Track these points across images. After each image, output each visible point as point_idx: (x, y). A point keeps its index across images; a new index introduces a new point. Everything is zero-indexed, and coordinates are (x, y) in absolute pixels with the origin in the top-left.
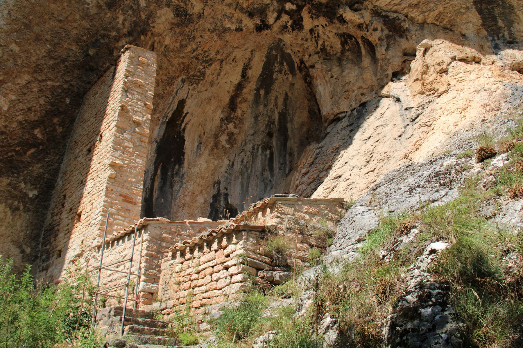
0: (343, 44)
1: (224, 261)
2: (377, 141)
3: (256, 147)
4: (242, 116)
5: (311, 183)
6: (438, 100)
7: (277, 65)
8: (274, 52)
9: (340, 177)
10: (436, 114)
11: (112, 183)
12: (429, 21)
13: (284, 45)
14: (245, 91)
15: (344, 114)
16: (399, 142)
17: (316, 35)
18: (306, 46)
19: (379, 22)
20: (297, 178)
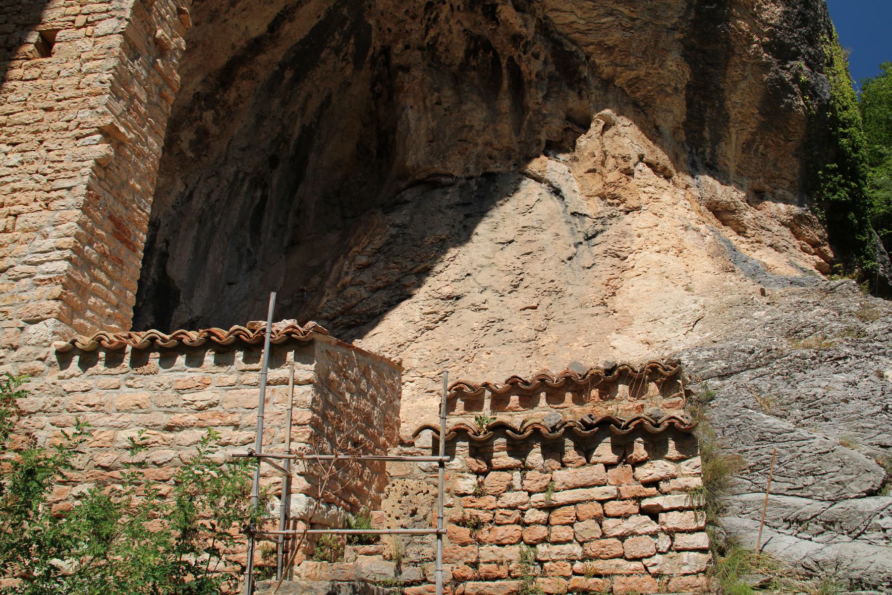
0: (470, 53)
1: (642, 494)
2: (528, 254)
3: (241, 176)
4: (236, 104)
5: (379, 289)
6: (628, 218)
7: (337, 37)
8: (345, 12)
9: (458, 298)
10: (632, 242)
11: (100, 179)
12: (618, 82)
13: (370, 6)
14: (262, 58)
15: (450, 180)
16: (570, 270)
17: (433, 16)
18: (408, 27)
19: (546, 47)
20: (345, 269)
